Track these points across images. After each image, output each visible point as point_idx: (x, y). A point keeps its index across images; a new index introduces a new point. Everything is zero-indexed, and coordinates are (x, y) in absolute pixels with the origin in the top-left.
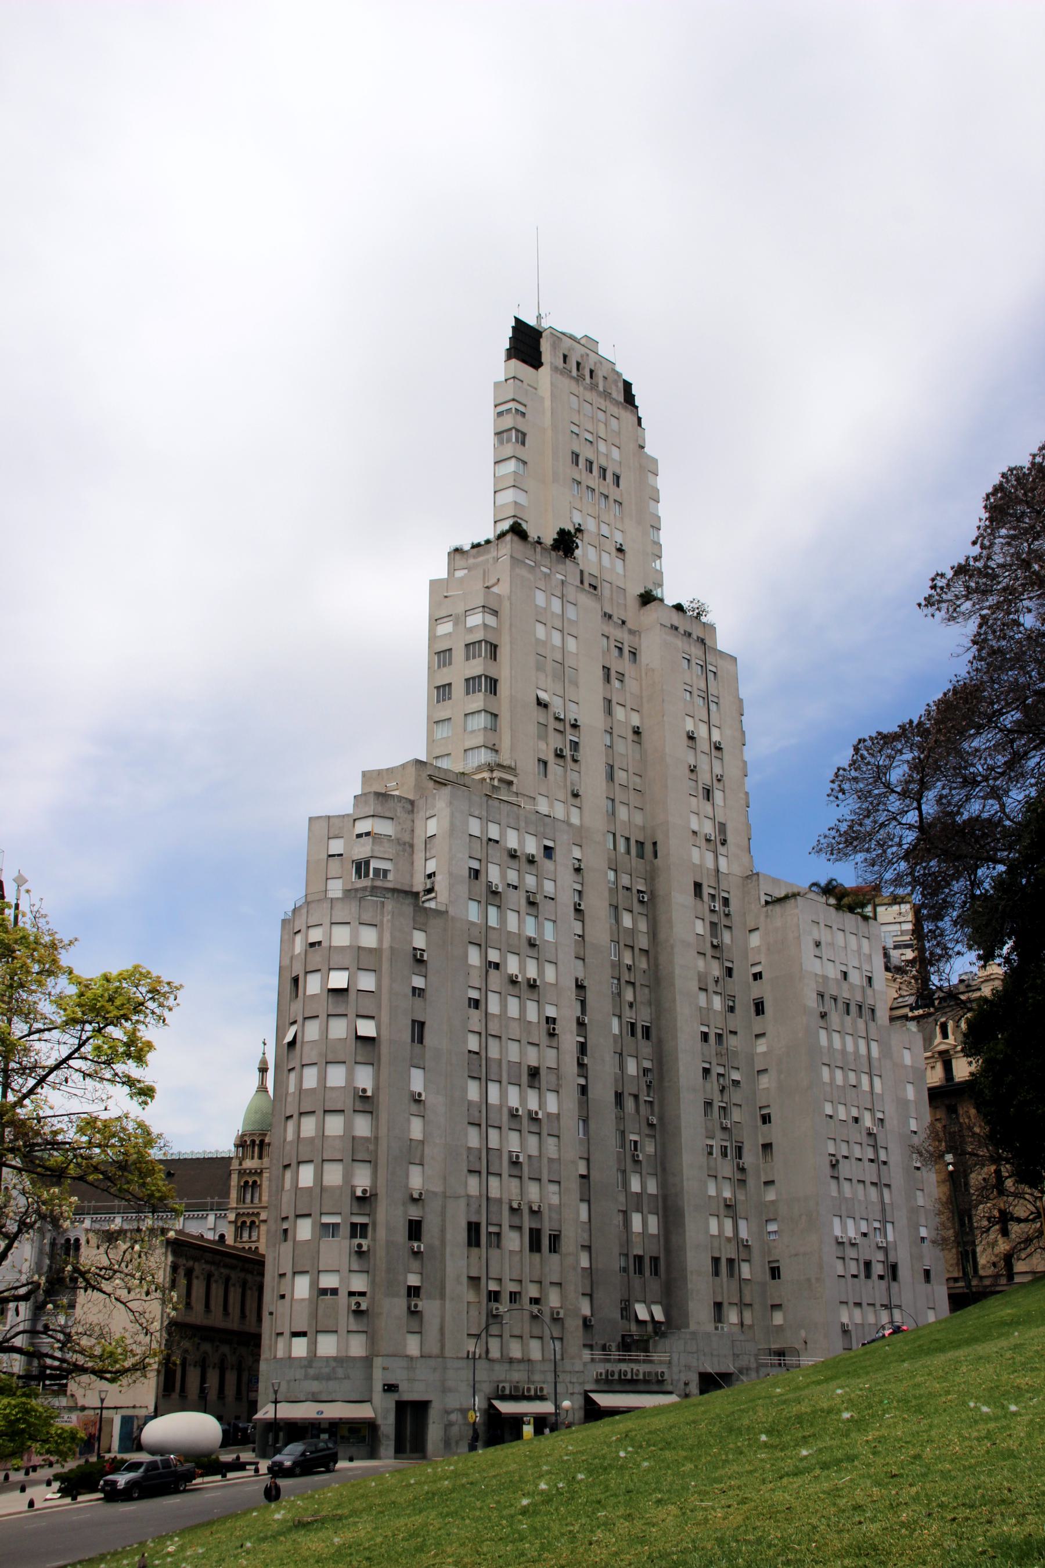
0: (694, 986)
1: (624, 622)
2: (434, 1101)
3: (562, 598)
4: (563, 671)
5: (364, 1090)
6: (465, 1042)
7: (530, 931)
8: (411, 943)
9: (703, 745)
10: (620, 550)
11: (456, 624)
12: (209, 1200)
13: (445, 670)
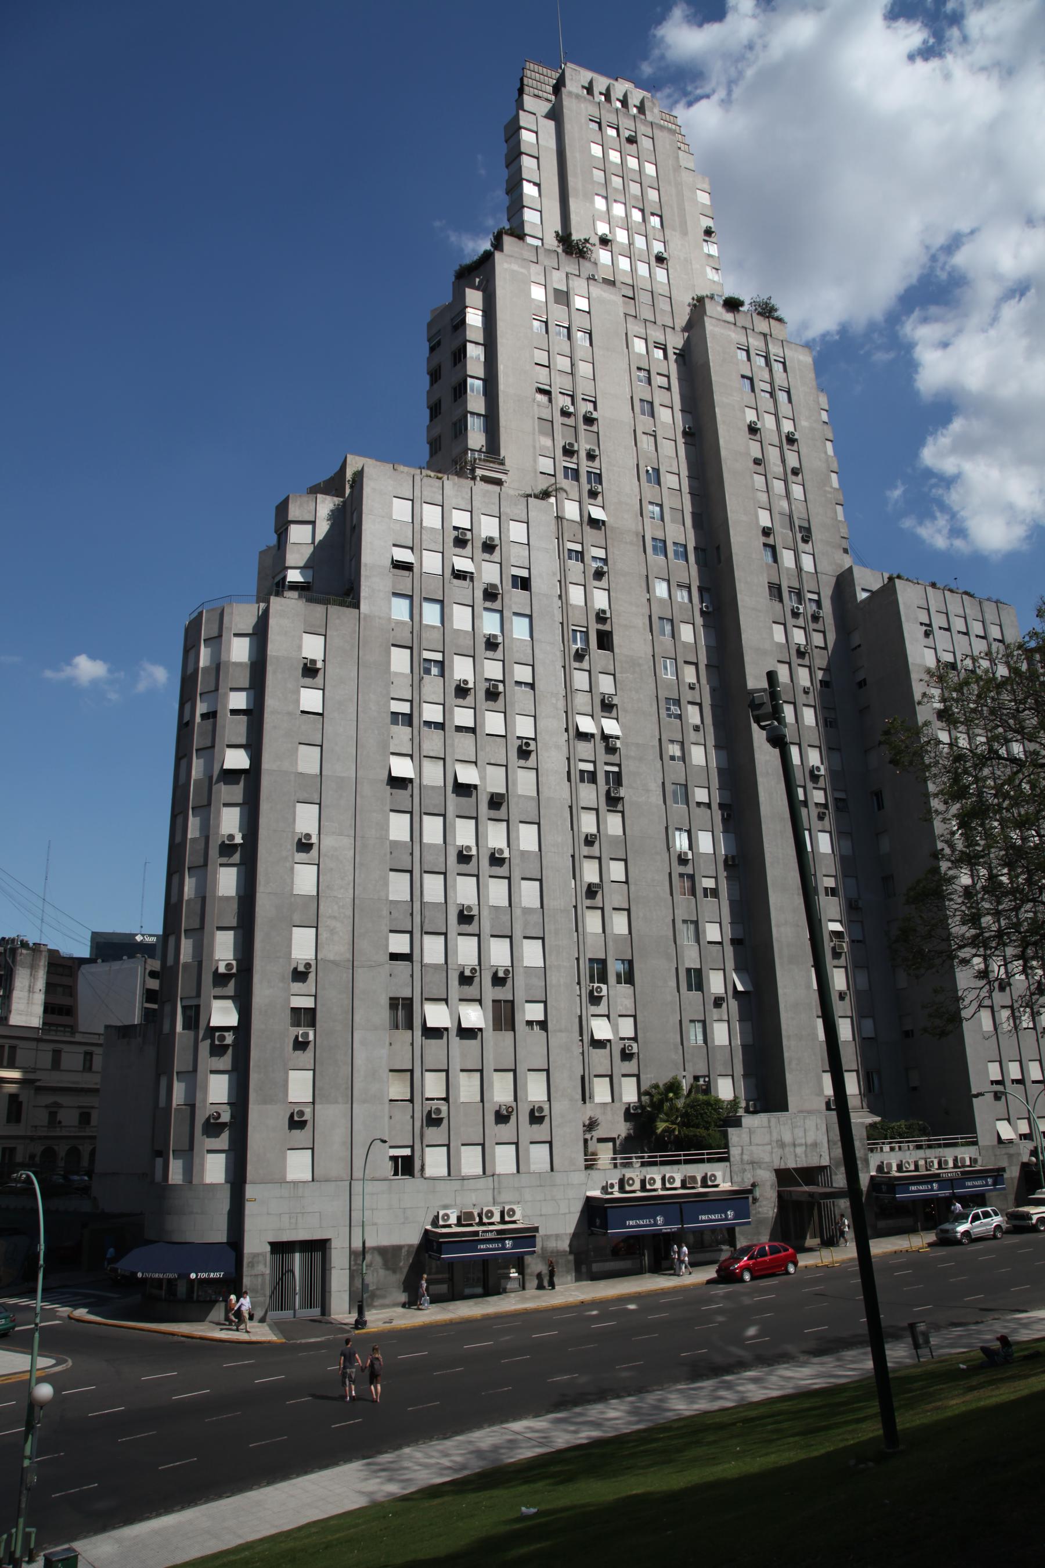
2: (335, 844)
7: (490, 624)
10: (660, 259)
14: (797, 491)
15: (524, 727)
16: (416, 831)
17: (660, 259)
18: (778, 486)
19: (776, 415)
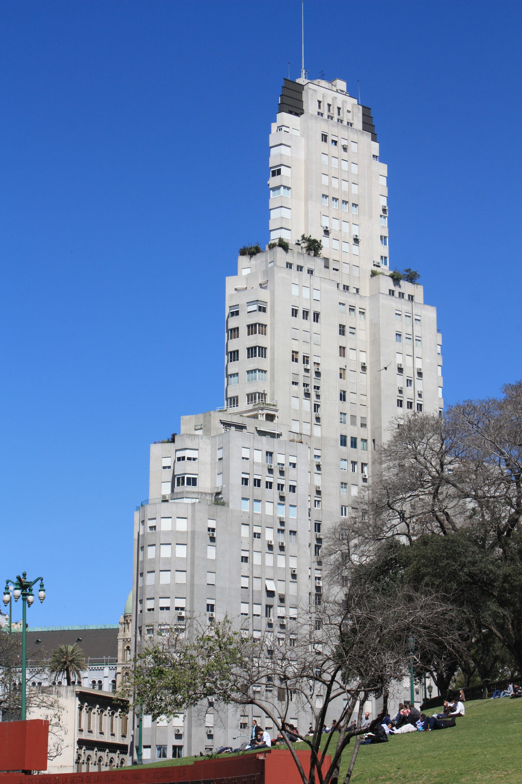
1: (357, 290)
6: (240, 582)
8: (207, 526)
9: (408, 372)
12: (104, 658)
13: (234, 341)
15: (293, 564)
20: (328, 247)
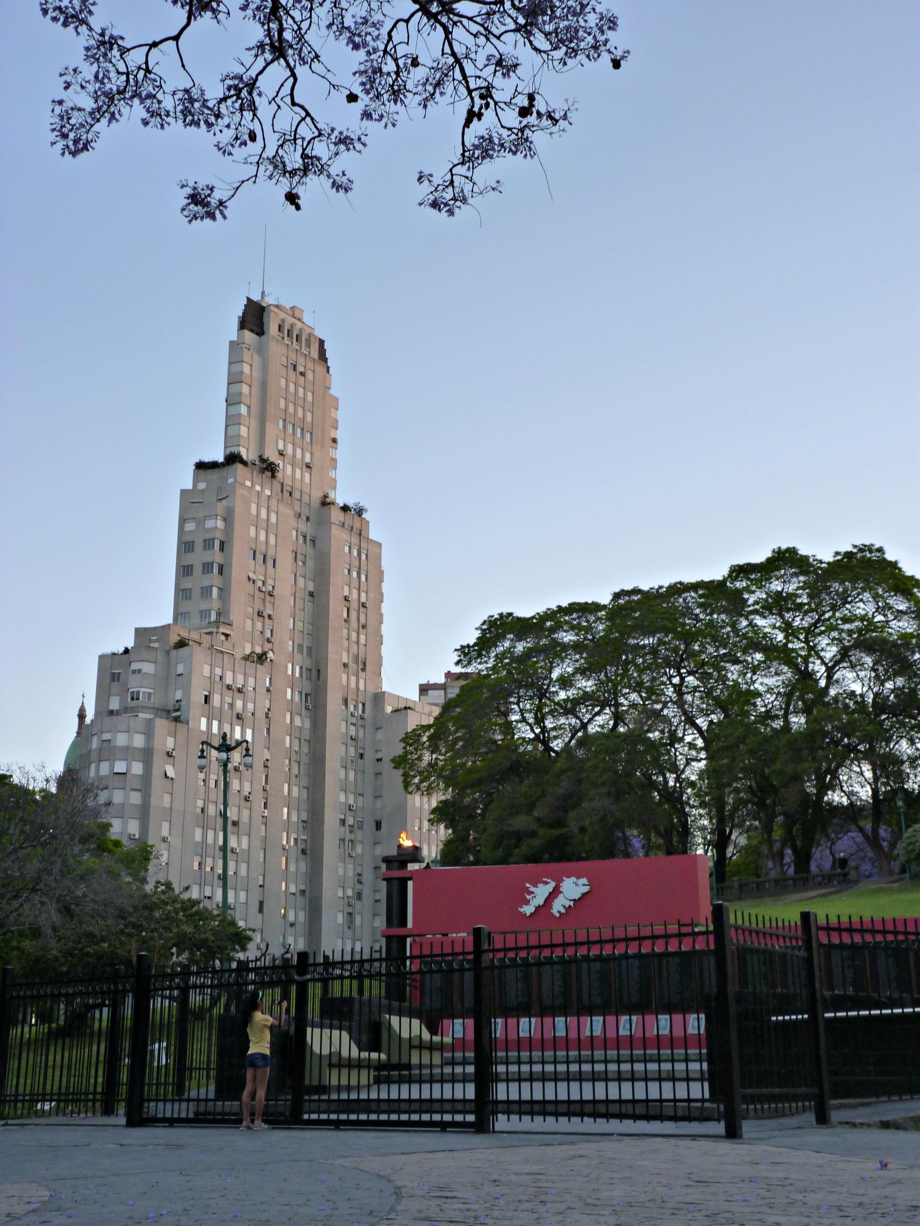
0: (338, 764)
1: (308, 519)
2: (175, 841)
3: (268, 508)
4: (267, 560)
5: (134, 835)
9: (354, 605)
10: (308, 466)
11: (197, 525)
13: (189, 555)
14: (362, 638)
16: (204, 836)
17: (308, 466)
18: (354, 635)
19: (359, 589)
20: (286, 470)
